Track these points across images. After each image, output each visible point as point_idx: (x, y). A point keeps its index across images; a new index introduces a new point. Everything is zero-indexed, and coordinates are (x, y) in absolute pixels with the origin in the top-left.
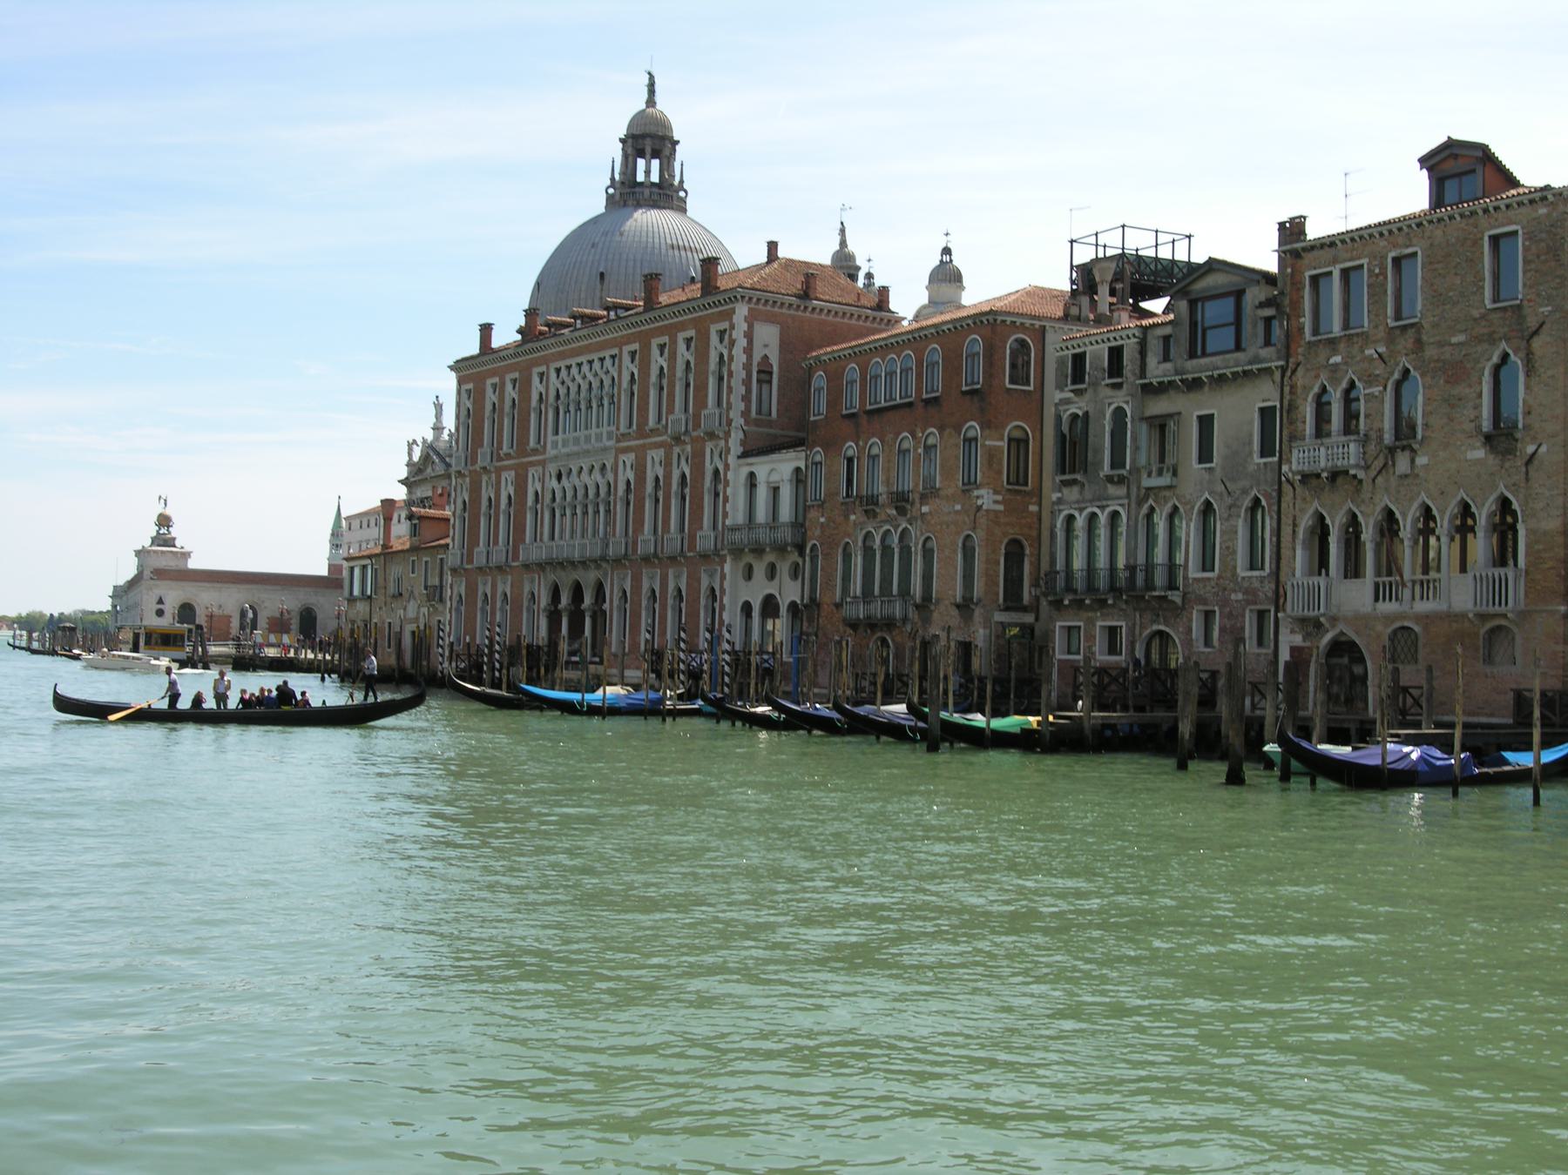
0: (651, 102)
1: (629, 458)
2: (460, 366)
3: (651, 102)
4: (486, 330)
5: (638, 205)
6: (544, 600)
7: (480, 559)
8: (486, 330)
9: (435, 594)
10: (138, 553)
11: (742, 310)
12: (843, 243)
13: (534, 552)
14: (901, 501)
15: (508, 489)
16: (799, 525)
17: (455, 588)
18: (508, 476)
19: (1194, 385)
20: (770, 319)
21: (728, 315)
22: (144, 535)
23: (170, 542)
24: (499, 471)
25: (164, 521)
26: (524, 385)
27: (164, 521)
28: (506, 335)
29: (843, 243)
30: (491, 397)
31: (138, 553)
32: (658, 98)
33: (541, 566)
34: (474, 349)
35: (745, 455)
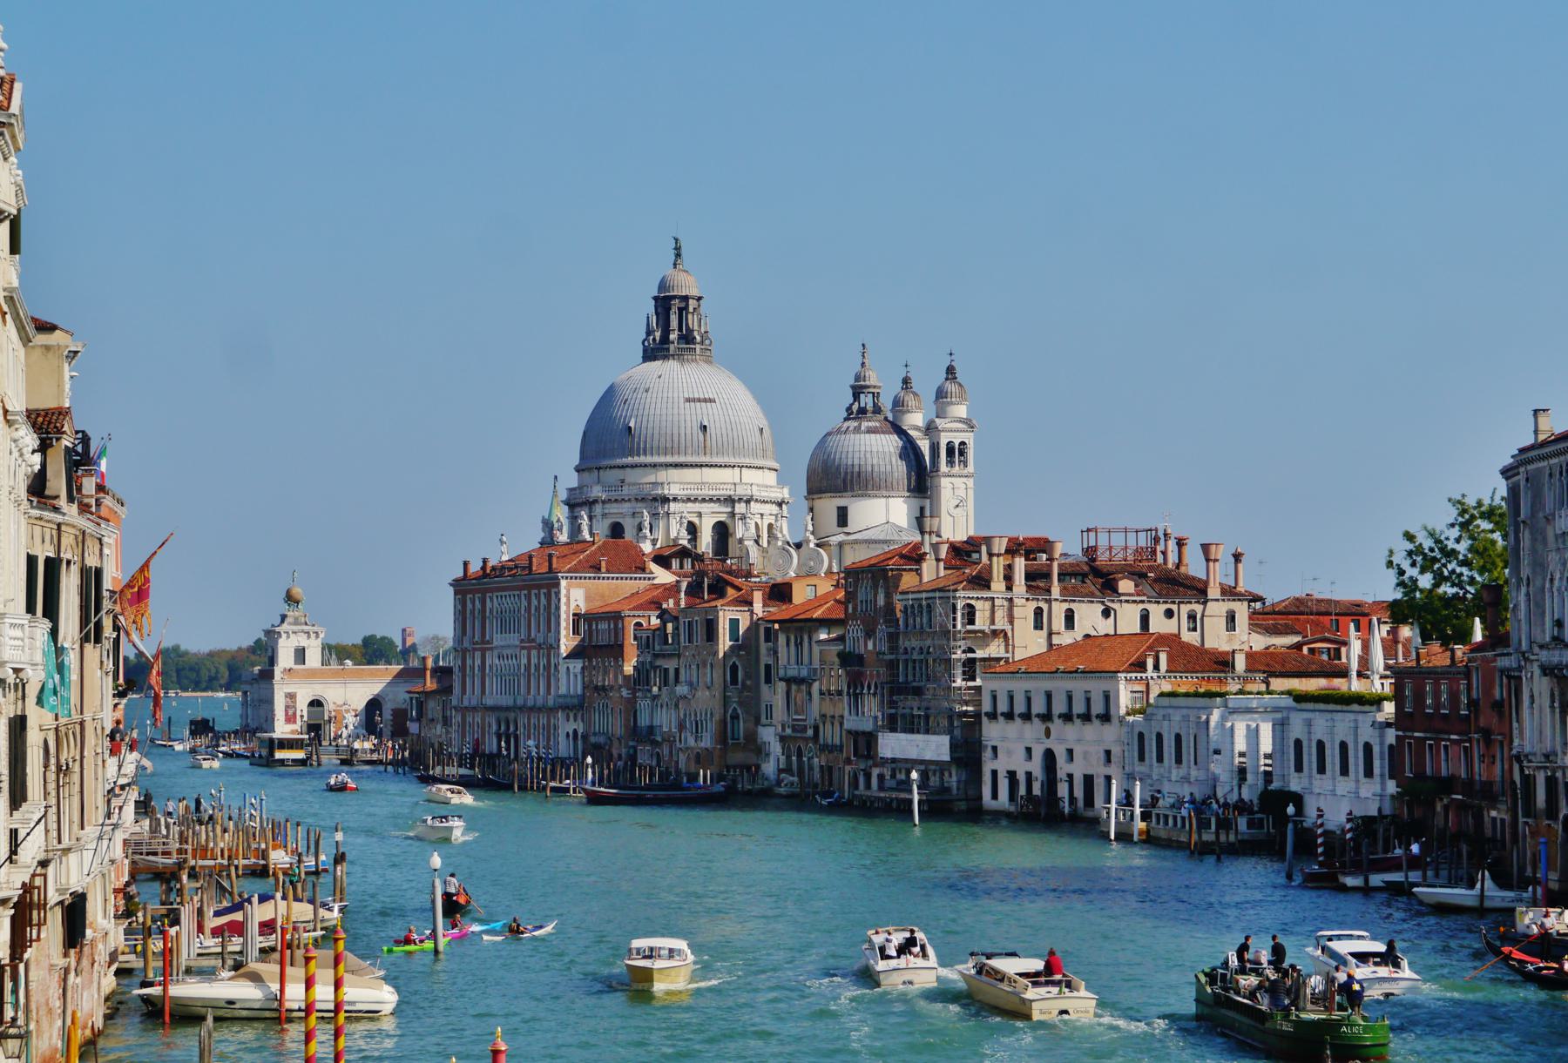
1: (525, 652)
4: (466, 564)
5: (666, 357)
6: (494, 728)
7: (466, 703)
8: (466, 564)
9: (446, 722)
11: (563, 583)
13: (489, 701)
14: (604, 688)
15: (478, 662)
16: (584, 695)
17: (457, 718)
18: (478, 654)
19: (664, 656)
20: (579, 586)
21: (558, 585)
24: (475, 650)
26: (483, 603)
28: (475, 567)
30: (469, 605)
34: (461, 574)
35: (567, 657)
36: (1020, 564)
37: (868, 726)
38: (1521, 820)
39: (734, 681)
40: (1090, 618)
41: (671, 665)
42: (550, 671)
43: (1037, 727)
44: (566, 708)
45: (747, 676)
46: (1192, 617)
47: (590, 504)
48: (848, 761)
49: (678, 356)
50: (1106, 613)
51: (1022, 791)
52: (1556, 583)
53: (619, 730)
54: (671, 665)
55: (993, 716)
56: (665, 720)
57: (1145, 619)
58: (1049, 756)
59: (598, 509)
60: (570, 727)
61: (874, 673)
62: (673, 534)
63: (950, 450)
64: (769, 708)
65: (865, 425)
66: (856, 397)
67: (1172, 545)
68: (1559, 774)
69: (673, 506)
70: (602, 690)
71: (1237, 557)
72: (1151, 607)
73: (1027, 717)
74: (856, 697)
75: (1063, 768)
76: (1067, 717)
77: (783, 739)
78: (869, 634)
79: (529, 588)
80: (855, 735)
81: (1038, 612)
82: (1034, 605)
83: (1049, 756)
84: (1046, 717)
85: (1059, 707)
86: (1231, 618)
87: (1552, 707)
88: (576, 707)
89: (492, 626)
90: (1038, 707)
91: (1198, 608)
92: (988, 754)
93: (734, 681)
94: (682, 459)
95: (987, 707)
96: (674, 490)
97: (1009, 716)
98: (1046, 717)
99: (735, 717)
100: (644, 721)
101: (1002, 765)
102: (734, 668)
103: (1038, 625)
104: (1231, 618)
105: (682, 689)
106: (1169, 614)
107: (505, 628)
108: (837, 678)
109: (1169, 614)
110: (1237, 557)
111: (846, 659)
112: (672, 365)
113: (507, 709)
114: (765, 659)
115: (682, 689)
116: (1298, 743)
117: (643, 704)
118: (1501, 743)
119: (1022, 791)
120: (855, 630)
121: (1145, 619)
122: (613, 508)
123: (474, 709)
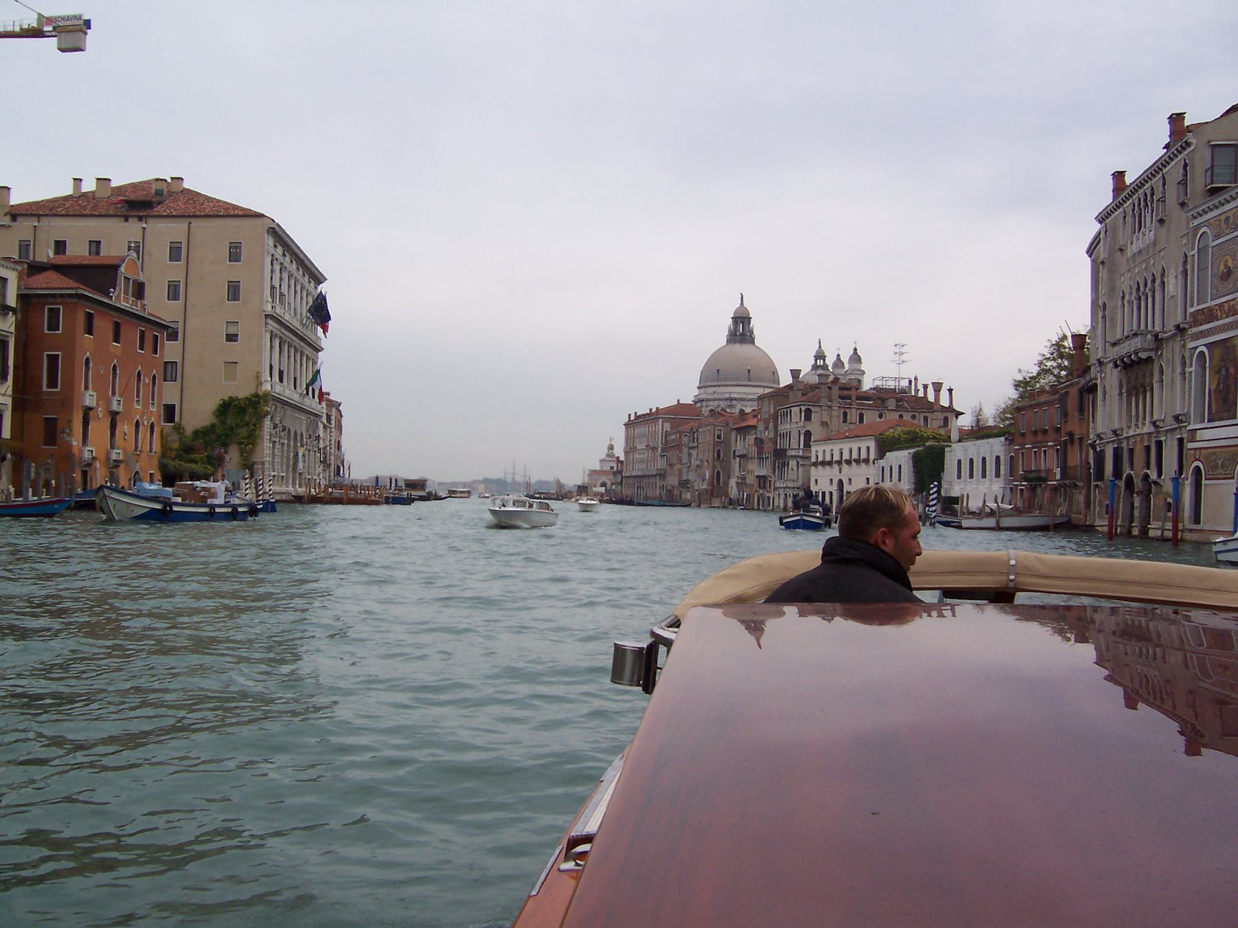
28: (632, 418)
37: (763, 472)
38: (1093, 483)
40: (871, 417)
43: (836, 467)
45: (725, 455)
46: (926, 419)
50: (881, 416)
52: (1127, 298)
55: (815, 464)
57: (901, 416)
58: (841, 482)
61: (768, 446)
67: (920, 388)
68: (1124, 444)
70: (671, 465)
71: (950, 390)
73: (830, 463)
74: (760, 459)
75: (846, 488)
76: (849, 462)
77: (737, 484)
78: (766, 428)
81: (845, 414)
83: (841, 482)
84: (839, 463)
87: (1121, 394)
89: (637, 441)
95: (813, 460)
96: (736, 396)
97: (823, 463)
98: (839, 463)
103: (845, 421)
105: (698, 463)
106: (914, 417)
108: (754, 451)
110: (950, 390)
112: (738, 346)
116: (959, 462)
118: (1081, 440)
120: (761, 427)
121: (901, 416)
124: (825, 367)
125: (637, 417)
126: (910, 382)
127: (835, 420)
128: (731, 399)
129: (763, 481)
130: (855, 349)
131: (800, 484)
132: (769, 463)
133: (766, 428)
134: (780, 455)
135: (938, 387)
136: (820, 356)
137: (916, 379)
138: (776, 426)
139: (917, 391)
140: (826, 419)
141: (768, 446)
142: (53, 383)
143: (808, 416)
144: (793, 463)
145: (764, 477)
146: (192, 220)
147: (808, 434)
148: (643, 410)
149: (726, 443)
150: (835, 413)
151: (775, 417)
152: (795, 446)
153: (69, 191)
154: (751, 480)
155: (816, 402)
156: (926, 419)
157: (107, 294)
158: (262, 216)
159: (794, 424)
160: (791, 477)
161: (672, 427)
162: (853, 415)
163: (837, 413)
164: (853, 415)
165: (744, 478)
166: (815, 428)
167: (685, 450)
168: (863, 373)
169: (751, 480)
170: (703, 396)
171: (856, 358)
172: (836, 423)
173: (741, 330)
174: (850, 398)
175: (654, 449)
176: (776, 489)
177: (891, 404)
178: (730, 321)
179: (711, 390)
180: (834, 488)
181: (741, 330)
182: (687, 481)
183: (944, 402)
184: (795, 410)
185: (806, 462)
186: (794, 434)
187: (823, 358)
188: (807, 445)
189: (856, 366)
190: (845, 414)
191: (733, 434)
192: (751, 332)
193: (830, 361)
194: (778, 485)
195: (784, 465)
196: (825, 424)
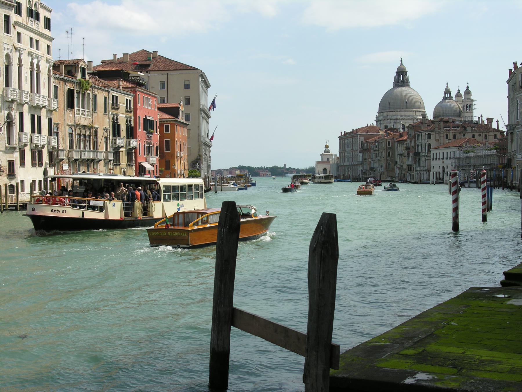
0: (401, 64)
2: (339, 137)
3: (401, 64)
4: (341, 133)
5: (398, 87)
8: (341, 133)
10: (321, 155)
12: (447, 87)
22: (322, 150)
23: (328, 152)
25: (327, 147)
27: (327, 147)
28: (343, 134)
29: (447, 87)
31: (321, 155)
32: (403, 63)
33: (346, 166)
36: (442, 124)
37: (410, 163)
39: (389, 155)
41: (377, 153)
42: (356, 156)
43: (441, 160)
44: (359, 164)
45: (392, 154)
46: (486, 136)
47: (380, 121)
48: (407, 172)
49: (402, 86)
51: (438, 177)
53: (368, 169)
54: (377, 153)
56: (376, 165)
57: (474, 136)
58: (443, 167)
59: (382, 122)
60: (361, 168)
61: (412, 151)
62: (399, 127)
63: (467, 107)
64: (397, 162)
65: (447, 101)
66: (445, 94)
69: (399, 121)
70: (365, 159)
71: (497, 122)
72: (475, 134)
75: (446, 170)
78: (411, 142)
79: (352, 137)
80: (408, 165)
81: (447, 135)
82: (445, 133)
83: (443, 167)
84: (443, 159)
85: (445, 156)
86: (495, 136)
88: (361, 164)
90: (441, 157)
91: (487, 134)
92: (432, 168)
93: (389, 155)
94: (401, 110)
96: (399, 117)
99: (389, 164)
100: (372, 166)
101: (435, 171)
102: (389, 153)
103: (447, 138)
104: (495, 136)
105: (378, 158)
106: (480, 135)
107: (348, 147)
109: (480, 135)
110: (497, 122)
111: (408, 148)
113: (348, 165)
114: (396, 150)
115: (378, 158)
117: (372, 162)
119: (438, 177)
120: (408, 141)
121: (474, 136)
122: (386, 122)
123: (343, 166)
124: (450, 98)
125: (346, 134)
126: (479, 118)
127: (442, 138)
128: (397, 119)
129: (410, 167)
130: (468, 87)
131: (426, 168)
132: (412, 159)
133: (411, 142)
134: (417, 154)
135: (490, 120)
136: (447, 91)
137: (481, 116)
138: (415, 142)
139: (483, 121)
140: (438, 138)
141: (412, 151)
142: (168, 149)
143: (429, 136)
144: (423, 159)
145: (410, 165)
146: (168, 72)
147: (429, 145)
148: (349, 130)
149: (393, 148)
150: (442, 135)
151: (415, 136)
152: (424, 150)
153: (112, 58)
154: (405, 167)
155: (432, 130)
156: (486, 136)
157: (178, 118)
158: (197, 69)
159: (423, 141)
160: (422, 165)
161: (365, 139)
162: (451, 136)
163: (443, 135)
164: (451, 136)
165: (402, 166)
166: (433, 142)
167: (372, 152)
168: (472, 101)
169: (405, 167)
170: (381, 118)
171: (468, 92)
172: (443, 139)
173: (401, 78)
174: (449, 127)
175: (356, 151)
176: (416, 171)
177: (469, 129)
178: (395, 74)
179: (385, 114)
180: (441, 170)
181: (401, 78)
182: (373, 168)
183: (494, 126)
184: (423, 134)
185: (429, 158)
186: (423, 146)
187: (450, 93)
188: (429, 151)
189: (467, 96)
190: (447, 135)
191: (396, 143)
192: (408, 81)
193: (453, 95)
194: (417, 169)
195: (420, 159)
196: (437, 140)
